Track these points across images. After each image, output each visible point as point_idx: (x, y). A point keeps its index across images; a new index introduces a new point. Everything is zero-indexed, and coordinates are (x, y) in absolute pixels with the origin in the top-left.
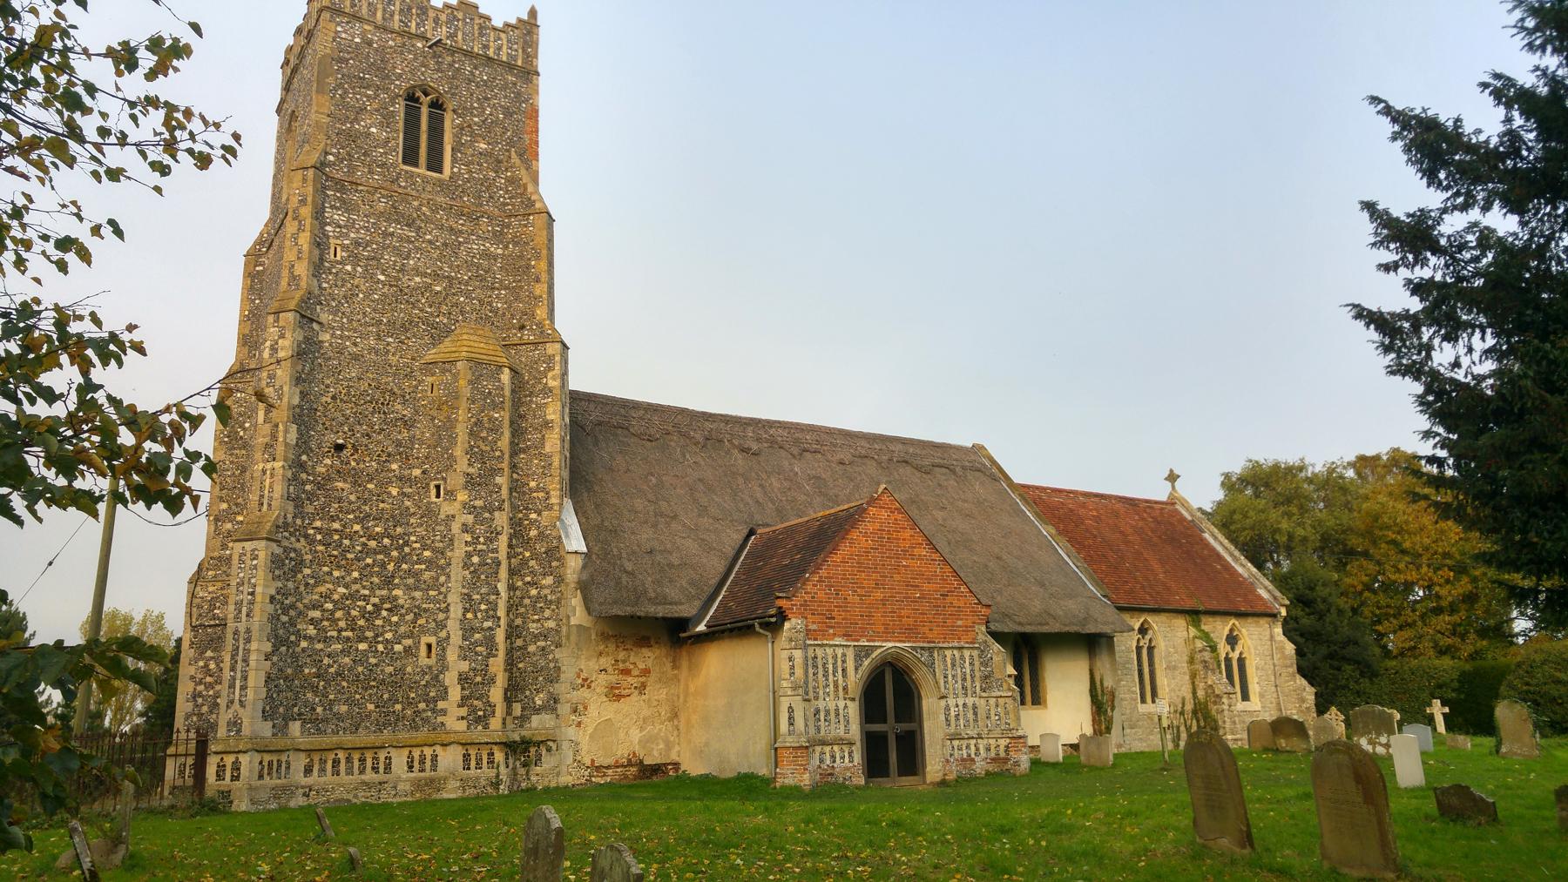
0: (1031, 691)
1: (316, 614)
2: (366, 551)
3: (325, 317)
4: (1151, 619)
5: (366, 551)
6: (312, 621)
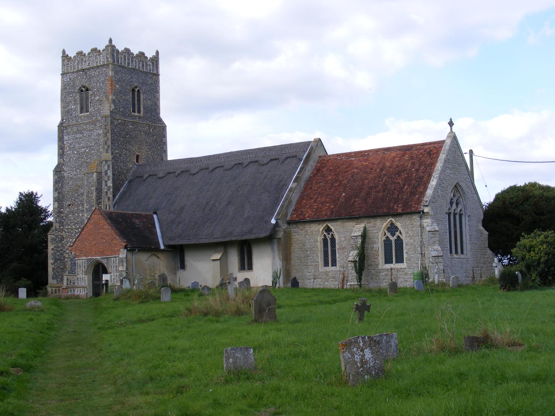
0: (246, 264)
1: (68, 251)
2: (76, 233)
3: (65, 169)
4: (331, 225)
5: (76, 233)
6: (67, 253)
